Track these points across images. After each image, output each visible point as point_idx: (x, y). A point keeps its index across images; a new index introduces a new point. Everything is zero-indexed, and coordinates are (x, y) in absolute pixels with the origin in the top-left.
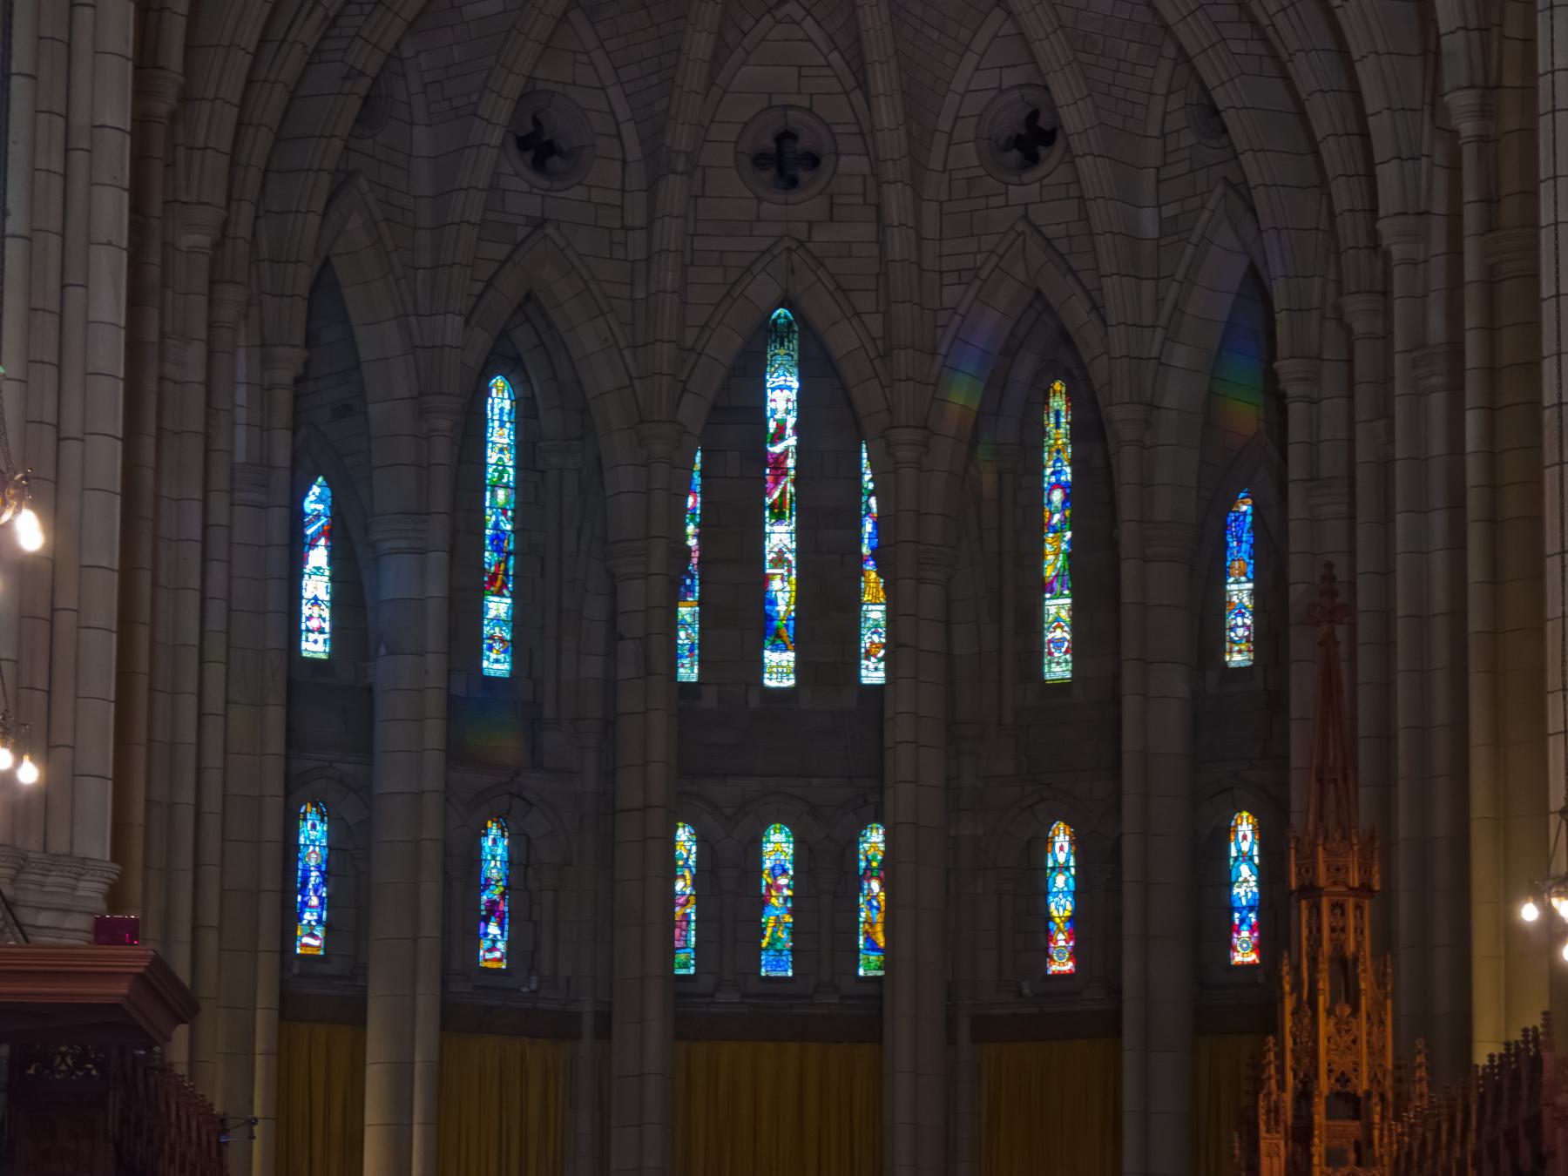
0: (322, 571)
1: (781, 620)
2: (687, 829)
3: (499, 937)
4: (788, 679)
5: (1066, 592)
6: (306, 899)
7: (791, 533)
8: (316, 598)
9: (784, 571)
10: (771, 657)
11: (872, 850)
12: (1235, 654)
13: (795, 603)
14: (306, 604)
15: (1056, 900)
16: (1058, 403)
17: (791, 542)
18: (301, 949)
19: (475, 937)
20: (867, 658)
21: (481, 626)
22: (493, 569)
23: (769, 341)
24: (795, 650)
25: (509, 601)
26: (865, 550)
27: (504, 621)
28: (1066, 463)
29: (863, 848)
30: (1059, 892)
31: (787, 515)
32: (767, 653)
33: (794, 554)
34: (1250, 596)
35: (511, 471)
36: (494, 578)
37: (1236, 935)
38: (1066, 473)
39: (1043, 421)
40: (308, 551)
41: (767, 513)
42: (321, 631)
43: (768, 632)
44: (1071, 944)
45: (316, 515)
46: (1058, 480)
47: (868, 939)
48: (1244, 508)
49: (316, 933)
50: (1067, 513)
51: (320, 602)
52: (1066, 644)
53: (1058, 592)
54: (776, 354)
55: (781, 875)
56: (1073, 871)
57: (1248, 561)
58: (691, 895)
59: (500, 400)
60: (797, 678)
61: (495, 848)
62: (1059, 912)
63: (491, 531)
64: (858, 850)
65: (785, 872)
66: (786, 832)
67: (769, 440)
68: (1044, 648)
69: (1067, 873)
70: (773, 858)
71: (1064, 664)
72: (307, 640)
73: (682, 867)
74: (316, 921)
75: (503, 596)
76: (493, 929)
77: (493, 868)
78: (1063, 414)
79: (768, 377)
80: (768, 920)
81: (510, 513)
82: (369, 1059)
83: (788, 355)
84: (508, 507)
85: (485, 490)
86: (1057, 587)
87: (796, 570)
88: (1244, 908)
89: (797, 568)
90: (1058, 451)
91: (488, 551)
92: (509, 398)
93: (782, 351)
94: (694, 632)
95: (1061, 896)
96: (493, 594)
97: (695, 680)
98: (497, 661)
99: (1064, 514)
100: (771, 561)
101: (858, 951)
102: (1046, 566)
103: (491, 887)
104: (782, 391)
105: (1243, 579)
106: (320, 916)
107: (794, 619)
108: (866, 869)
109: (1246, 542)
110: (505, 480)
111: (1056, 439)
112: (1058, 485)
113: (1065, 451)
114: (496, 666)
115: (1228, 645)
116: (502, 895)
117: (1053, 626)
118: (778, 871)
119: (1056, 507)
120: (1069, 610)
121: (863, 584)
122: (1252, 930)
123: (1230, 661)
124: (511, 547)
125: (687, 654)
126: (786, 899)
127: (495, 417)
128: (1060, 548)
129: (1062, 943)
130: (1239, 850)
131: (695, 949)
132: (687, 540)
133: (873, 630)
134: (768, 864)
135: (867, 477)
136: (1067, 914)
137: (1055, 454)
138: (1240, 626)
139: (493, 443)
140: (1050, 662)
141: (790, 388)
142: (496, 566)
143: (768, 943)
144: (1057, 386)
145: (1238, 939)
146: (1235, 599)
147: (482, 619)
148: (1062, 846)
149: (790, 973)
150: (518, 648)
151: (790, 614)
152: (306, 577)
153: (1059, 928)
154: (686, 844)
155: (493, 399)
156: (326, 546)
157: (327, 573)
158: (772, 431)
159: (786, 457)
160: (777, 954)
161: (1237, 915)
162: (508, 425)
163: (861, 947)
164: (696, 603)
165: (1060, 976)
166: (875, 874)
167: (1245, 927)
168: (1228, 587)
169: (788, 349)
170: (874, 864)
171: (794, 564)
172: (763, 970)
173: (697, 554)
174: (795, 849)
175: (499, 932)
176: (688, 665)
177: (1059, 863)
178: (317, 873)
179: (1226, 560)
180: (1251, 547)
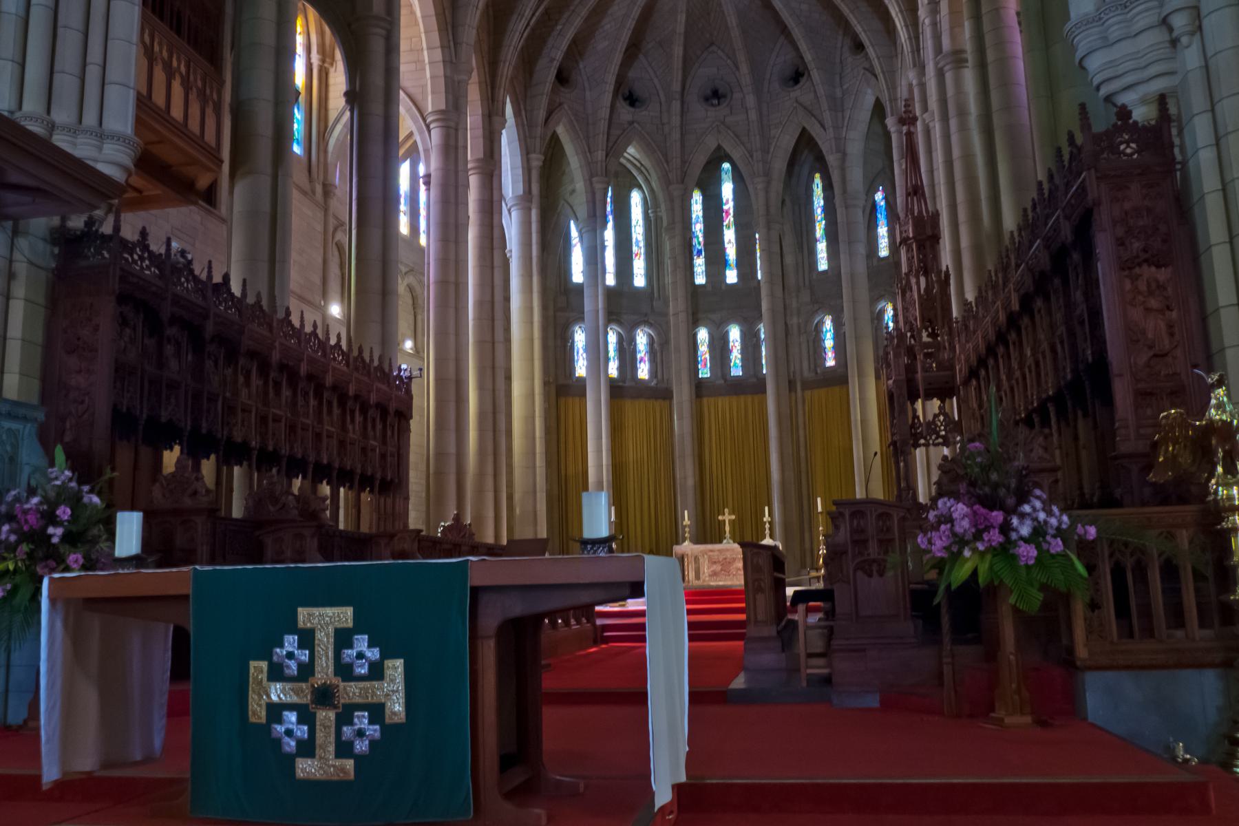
56: (832, 331)
59: (636, 198)
61: (642, 340)
65: (737, 341)
86: (821, 240)
112: (819, 207)
116: (645, 355)
134: (731, 339)
146: (881, 234)
148: (828, 324)
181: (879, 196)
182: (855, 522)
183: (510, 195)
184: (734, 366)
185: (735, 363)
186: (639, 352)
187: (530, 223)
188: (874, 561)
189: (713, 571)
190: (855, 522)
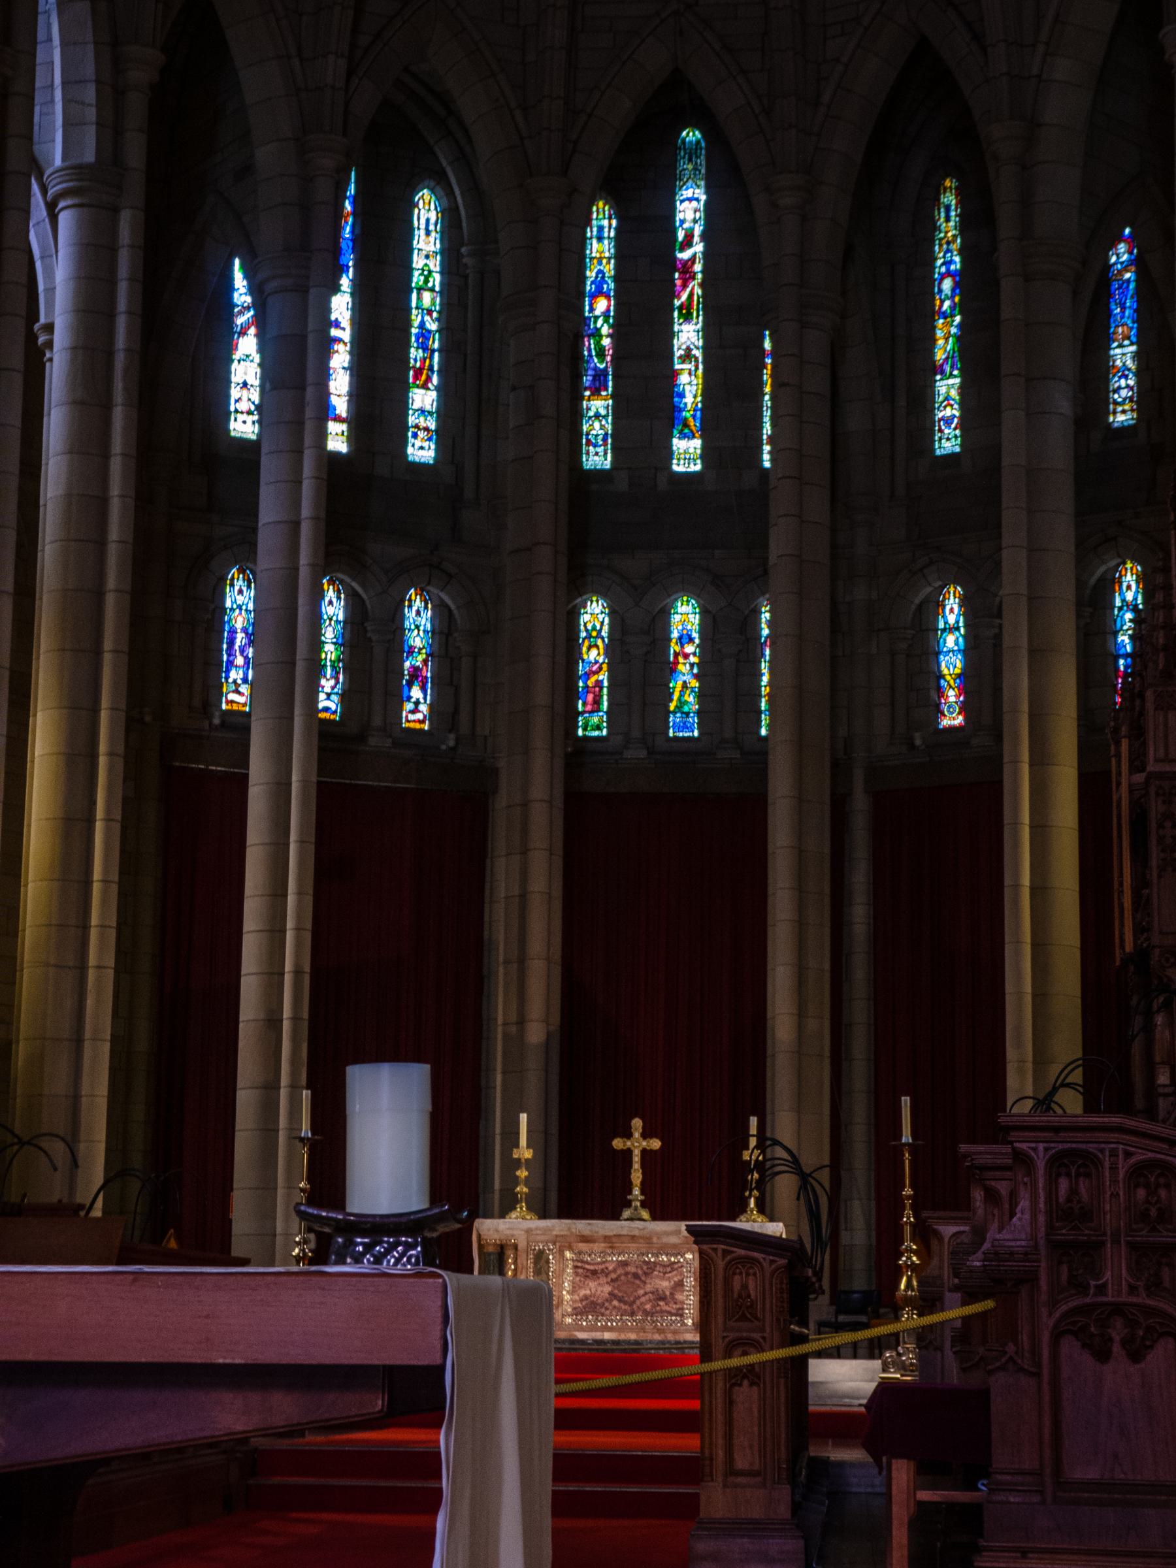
1: (689, 411)
3: (422, 701)
4: (695, 465)
6: (232, 658)
7: (698, 331)
8: (245, 384)
9: (692, 366)
10: (679, 445)
12: (1118, 415)
13: (702, 395)
15: (947, 658)
17: (698, 339)
18: (227, 705)
19: (400, 698)
21: (405, 416)
24: (702, 437)
27: (429, 412)
28: (955, 253)
30: (949, 651)
31: (695, 314)
32: (675, 441)
33: (701, 350)
34: (1133, 358)
36: (418, 373)
38: (955, 263)
39: (934, 217)
41: (676, 314)
43: (676, 422)
44: (961, 699)
48: (1128, 275)
49: (240, 689)
50: (957, 299)
52: (956, 420)
53: (948, 374)
54: (684, 170)
55: (688, 643)
57: (1131, 325)
58: (604, 663)
60: (703, 463)
62: (949, 670)
64: (761, 619)
65: (691, 640)
66: (693, 605)
67: (677, 247)
69: (957, 633)
70: (680, 628)
71: (953, 439)
72: (236, 420)
75: (428, 389)
76: (416, 693)
78: (953, 207)
80: (676, 685)
84: (433, 309)
86: (948, 369)
89: (704, 363)
94: (608, 423)
95: (951, 654)
96: (418, 387)
97: (608, 467)
98: (422, 448)
99: (953, 301)
100: (680, 357)
102: (936, 350)
103: (414, 655)
105: (1126, 342)
109: (1130, 307)
111: (946, 232)
112: (948, 274)
113: (954, 241)
114: (421, 453)
115: (1111, 407)
116: (425, 662)
117: (943, 405)
118: (685, 640)
119: (946, 295)
120: (959, 388)
123: (1114, 421)
126: (692, 665)
128: (950, 332)
130: (1123, 600)
134: (675, 635)
136: (958, 671)
137: (945, 246)
138: (1124, 387)
139: (419, 250)
140: (940, 439)
141: (697, 200)
142: (421, 361)
143: (676, 707)
146: (1118, 363)
147: (408, 409)
148: (952, 611)
149: (696, 734)
150: (444, 436)
151: (697, 405)
154: (599, 616)
155: (419, 210)
160: (684, 716)
161: (1122, 662)
163: (763, 708)
165: (951, 729)
169: (696, 163)
171: (700, 360)
172: (671, 731)
173: (611, 352)
174: (701, 620)
176: (602, 454)
177: (949, 625)
178: (244, 635)
179: (1109, 328)
181: (1121, 254)
182: (1064, 1185)
183: (58, 162)
184: (679, 708)
185: (682, 703)
187: (113, 250)
188: (1117, 1309)
189: (586, 1297)
190: (1064, 1185)
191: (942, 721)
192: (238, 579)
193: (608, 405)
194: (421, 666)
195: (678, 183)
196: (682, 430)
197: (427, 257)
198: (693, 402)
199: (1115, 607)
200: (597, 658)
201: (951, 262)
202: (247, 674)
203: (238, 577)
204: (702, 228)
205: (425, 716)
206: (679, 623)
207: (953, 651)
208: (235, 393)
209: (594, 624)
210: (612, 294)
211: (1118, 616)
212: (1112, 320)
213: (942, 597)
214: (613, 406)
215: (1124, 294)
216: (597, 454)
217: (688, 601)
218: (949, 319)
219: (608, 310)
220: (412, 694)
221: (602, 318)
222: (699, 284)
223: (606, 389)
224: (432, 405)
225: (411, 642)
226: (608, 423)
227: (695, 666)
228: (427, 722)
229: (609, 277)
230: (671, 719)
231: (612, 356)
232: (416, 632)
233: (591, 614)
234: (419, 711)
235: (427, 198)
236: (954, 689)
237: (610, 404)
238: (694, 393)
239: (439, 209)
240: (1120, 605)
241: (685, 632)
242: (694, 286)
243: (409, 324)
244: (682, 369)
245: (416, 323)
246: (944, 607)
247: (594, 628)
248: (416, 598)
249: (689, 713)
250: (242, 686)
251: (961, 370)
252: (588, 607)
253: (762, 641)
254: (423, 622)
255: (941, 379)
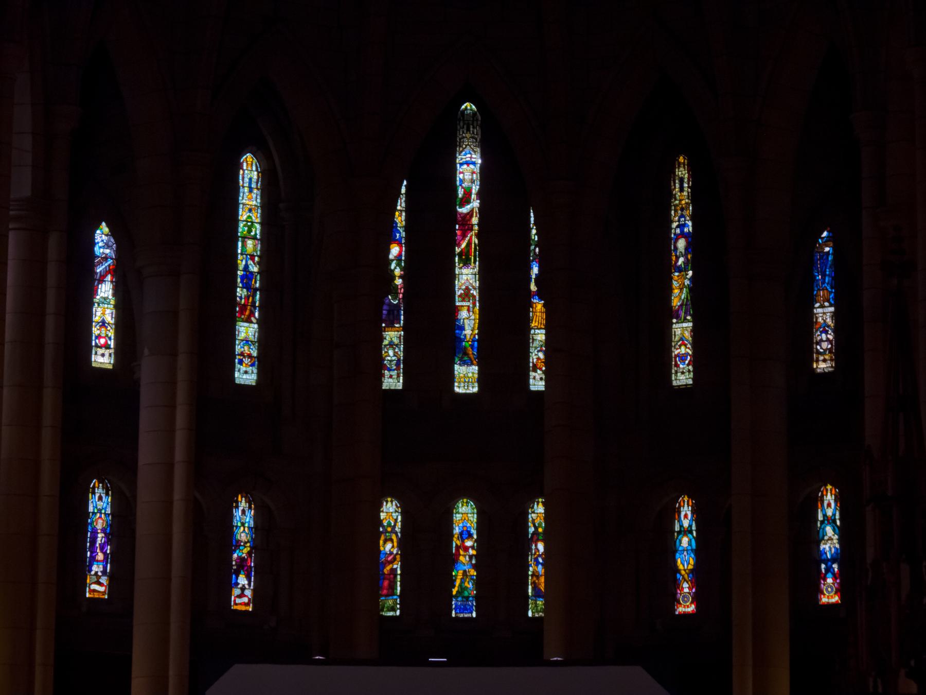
0: (108, 300)
1: (468, 342)
2: (394, 503)
3: (247, 587)
4: (473, 387)
5: (689, 318)
7: (475, 274)
9: (470, 304)
10: (460, 370)
11: (539, 518)
12: (820, 363)
13: (478, 329)
14: (95, 326)
16: (682, 172)
17: (476, 281)
18: (90, 594)
19: (230, 586)
20: (535, 371)
22: (243, 301)
23: (459, 127)
24: (478, 365)
25: (256, 326)
26: (533, 287)
27: (252, 341)
28: (688, 218)
29: (532, 518)
30: (684, 550)
31: (472, 260)
32: (456, 367)
33: (478, 291)
34: (832, 317)
35: (258, 226)
37: (822, 582)
38: (688, 226)
39: (671, 186)
40: (98, 285)
41: (457, 259)
42: (107, 346)
45: (104, 258)
46: (682, 231)
47: (535, 587)
48: (827, 249)
49: (101, 580)
50: (689, 257)
51: (106, 325)
52: (689, 358)
54: (464, 138)
55: (467, 538)
58: (397, 554)
60: (479, 387)
63: (242, 272)
64: (528, 518)
65: (470, 536)
66: (471, 506)
67: (458, 203)
68: (672, 361)
69: (690, 536)
70: (461, 525)
72: (96, 353)
73: (390, 532)
74: (101, 572)
75: (251, 322)
76: (242, 580)
77: (242, 532)
78: (686, 180)
79: (457, 155)
80: (458, 574)
81: (256, 259)
82: (134, 674)
83: (473, 138)
84: (255, 254)
85: (237, 241)
87: (479, 303)
88: (828, 560)
90: (682, 209)
91: (239, 287)
92: (257, 170)
93: (468, 135)
94: (400, 351)
95: (685, 553)
96: (243, 321)
98: (246, 372)
99: (686, 258)
100: (460, 296)
101: (527, 597)
103: (241, 548)
104: (468, 166)
105: (826, 304)
106: (105, 568)
107: (478, 341)
108: (533, 534)
110: (253, 234)
111: (680, 200)
112: (683, 235)
113: (687, 208)
114: (245, 376)
116: (249, 553)
119: (681, 252)
120: (692, 331)
121: (531, 313)
122: (835, 577)
123: (817, 367)
124: (258, 285)
125: (395, 367)
126: (471, 557)
127: (245, 185)
128: (684, 284)
129: (686, 590)
130: (825, 515)
131: (400, 596)
132: (395, 280)
133: (539, 349)
134: (457, 531)
135: (534, 231)
136: (690, 567)
137: (679, 212)
138: (825, 340)
139: (244, 204)
140: (676, 372)
141: (474, 163)
142: (245, 298)
143: (458, 592)
144: (681, 159)
145: (824, 585)
146: (820, 320)
147: (235, 339)
148: (686, 516)
149: (474, 615)
150: (263, 362)
151: (474, 337)
152: (96, 305)
153: (683, 578)
154: (394, 514)
155: (244, 170)
156: (112, 282)
157: (113, 302)
158: (460, 196)
159: (472, 216)
160: (464, 599)
161: (823, 566)
162: (255, 191)
163: (530, 594)
164: (401, 329)
165: (685, 615)
166: (541, 538)
167: (829, 575)
168: (815, 311)
169: (473, 133)
170: (540, 530)
171: (477, 299)
172: (454, 612)
173: (402, 290)
175: (246, 582)
176: (396, 376)
178: (103, 535)
180: (832, 280)
185: (462, 589)
186: (238, 545)
191: (678, 608)
192: (98, 488)
193: (400, 335)
194: (246, 557)
195: (458, 149)
196: (462, 358)
197: (250, 210)
198: (472, 334)
199: (818, 520)
200: (392, 550)
201: (684, 225)
202: (107, 567)
203: (99, 486)
204: (478, 187)
205: (249, 599)
206: (460, 522)
207: (687, 550)
208: (95, 331)
209: (389, 521)
210: (403, 241)
211: (820, 528)
212: (815, 284)
213: (678, 504)
214: (404, 336)
215: (824, 264)
216: (391, 377)
217: (467, 503)
218: (683, 273)
219: (400, 254)
220: (239, 581)
221: (395, 261)
222: (475, 235)
223: (399, 323)
224: (254, 336)
225: (238, 537)
226: (400, 351)
227: (474, 557)
228: (251, 605)
229: (400, 227)
230: (453, 603)
231: (403, 294)
232: (242, 529)
233: (387, 513)
234: (245, 596)
235: (250, 160)
236: (687, 583)
237: (402, 335)
238: (472, 326)
239: (259, 169)
240: (822, 519)
241: (465, 529)
242: (472, 235)
243: (236, 267)
244: (462, 306)
245: (241, 267)
246: (679, 513)
247: (389, 525)
248: (242, 500)
249: (468, 597)
250: (103, 578)
251: (691, 316)
252: (384, 507)
253: (530, 537)
254: (247, 520)
255: (677, 323)
